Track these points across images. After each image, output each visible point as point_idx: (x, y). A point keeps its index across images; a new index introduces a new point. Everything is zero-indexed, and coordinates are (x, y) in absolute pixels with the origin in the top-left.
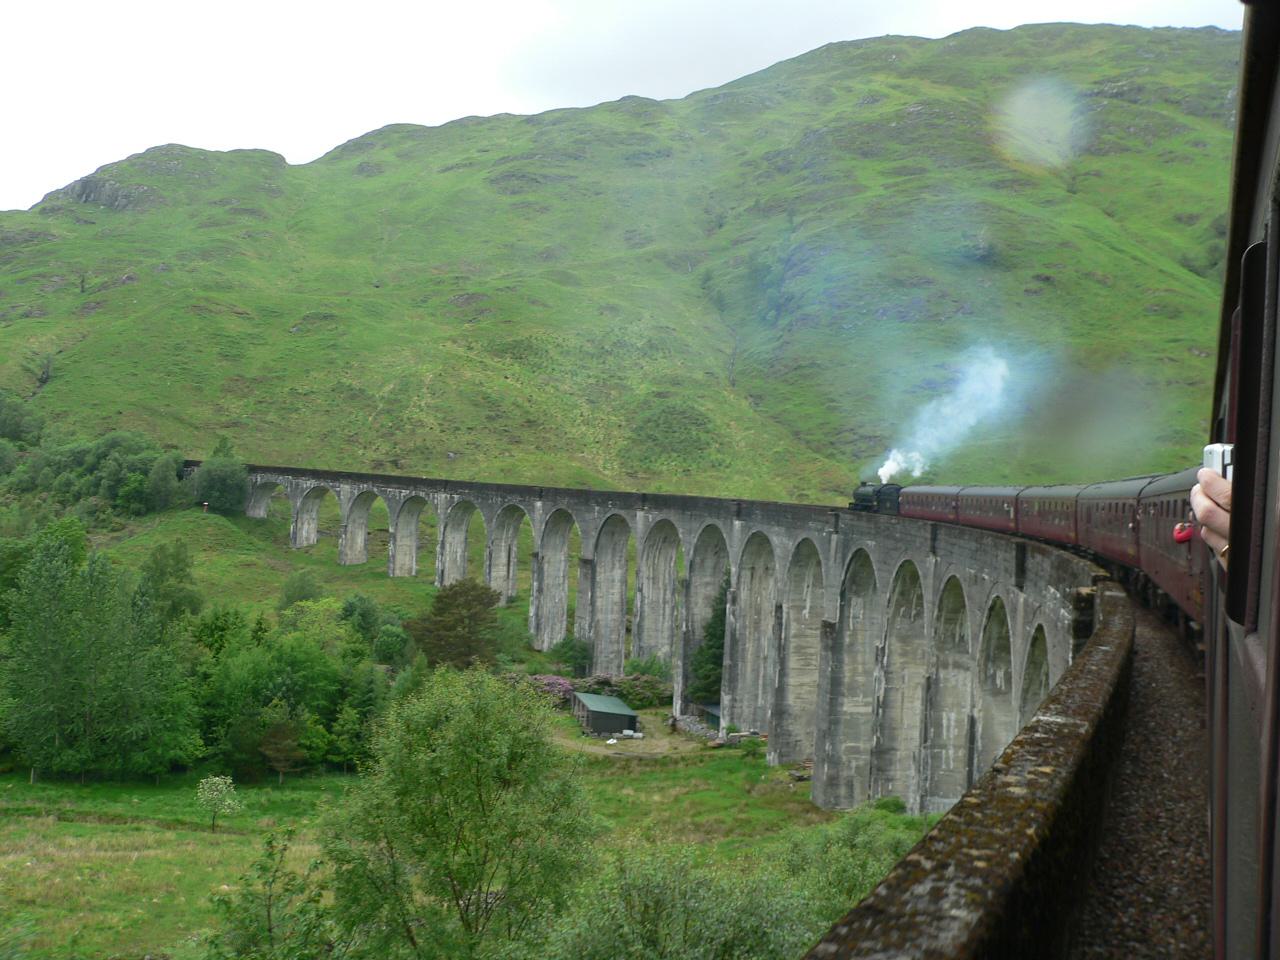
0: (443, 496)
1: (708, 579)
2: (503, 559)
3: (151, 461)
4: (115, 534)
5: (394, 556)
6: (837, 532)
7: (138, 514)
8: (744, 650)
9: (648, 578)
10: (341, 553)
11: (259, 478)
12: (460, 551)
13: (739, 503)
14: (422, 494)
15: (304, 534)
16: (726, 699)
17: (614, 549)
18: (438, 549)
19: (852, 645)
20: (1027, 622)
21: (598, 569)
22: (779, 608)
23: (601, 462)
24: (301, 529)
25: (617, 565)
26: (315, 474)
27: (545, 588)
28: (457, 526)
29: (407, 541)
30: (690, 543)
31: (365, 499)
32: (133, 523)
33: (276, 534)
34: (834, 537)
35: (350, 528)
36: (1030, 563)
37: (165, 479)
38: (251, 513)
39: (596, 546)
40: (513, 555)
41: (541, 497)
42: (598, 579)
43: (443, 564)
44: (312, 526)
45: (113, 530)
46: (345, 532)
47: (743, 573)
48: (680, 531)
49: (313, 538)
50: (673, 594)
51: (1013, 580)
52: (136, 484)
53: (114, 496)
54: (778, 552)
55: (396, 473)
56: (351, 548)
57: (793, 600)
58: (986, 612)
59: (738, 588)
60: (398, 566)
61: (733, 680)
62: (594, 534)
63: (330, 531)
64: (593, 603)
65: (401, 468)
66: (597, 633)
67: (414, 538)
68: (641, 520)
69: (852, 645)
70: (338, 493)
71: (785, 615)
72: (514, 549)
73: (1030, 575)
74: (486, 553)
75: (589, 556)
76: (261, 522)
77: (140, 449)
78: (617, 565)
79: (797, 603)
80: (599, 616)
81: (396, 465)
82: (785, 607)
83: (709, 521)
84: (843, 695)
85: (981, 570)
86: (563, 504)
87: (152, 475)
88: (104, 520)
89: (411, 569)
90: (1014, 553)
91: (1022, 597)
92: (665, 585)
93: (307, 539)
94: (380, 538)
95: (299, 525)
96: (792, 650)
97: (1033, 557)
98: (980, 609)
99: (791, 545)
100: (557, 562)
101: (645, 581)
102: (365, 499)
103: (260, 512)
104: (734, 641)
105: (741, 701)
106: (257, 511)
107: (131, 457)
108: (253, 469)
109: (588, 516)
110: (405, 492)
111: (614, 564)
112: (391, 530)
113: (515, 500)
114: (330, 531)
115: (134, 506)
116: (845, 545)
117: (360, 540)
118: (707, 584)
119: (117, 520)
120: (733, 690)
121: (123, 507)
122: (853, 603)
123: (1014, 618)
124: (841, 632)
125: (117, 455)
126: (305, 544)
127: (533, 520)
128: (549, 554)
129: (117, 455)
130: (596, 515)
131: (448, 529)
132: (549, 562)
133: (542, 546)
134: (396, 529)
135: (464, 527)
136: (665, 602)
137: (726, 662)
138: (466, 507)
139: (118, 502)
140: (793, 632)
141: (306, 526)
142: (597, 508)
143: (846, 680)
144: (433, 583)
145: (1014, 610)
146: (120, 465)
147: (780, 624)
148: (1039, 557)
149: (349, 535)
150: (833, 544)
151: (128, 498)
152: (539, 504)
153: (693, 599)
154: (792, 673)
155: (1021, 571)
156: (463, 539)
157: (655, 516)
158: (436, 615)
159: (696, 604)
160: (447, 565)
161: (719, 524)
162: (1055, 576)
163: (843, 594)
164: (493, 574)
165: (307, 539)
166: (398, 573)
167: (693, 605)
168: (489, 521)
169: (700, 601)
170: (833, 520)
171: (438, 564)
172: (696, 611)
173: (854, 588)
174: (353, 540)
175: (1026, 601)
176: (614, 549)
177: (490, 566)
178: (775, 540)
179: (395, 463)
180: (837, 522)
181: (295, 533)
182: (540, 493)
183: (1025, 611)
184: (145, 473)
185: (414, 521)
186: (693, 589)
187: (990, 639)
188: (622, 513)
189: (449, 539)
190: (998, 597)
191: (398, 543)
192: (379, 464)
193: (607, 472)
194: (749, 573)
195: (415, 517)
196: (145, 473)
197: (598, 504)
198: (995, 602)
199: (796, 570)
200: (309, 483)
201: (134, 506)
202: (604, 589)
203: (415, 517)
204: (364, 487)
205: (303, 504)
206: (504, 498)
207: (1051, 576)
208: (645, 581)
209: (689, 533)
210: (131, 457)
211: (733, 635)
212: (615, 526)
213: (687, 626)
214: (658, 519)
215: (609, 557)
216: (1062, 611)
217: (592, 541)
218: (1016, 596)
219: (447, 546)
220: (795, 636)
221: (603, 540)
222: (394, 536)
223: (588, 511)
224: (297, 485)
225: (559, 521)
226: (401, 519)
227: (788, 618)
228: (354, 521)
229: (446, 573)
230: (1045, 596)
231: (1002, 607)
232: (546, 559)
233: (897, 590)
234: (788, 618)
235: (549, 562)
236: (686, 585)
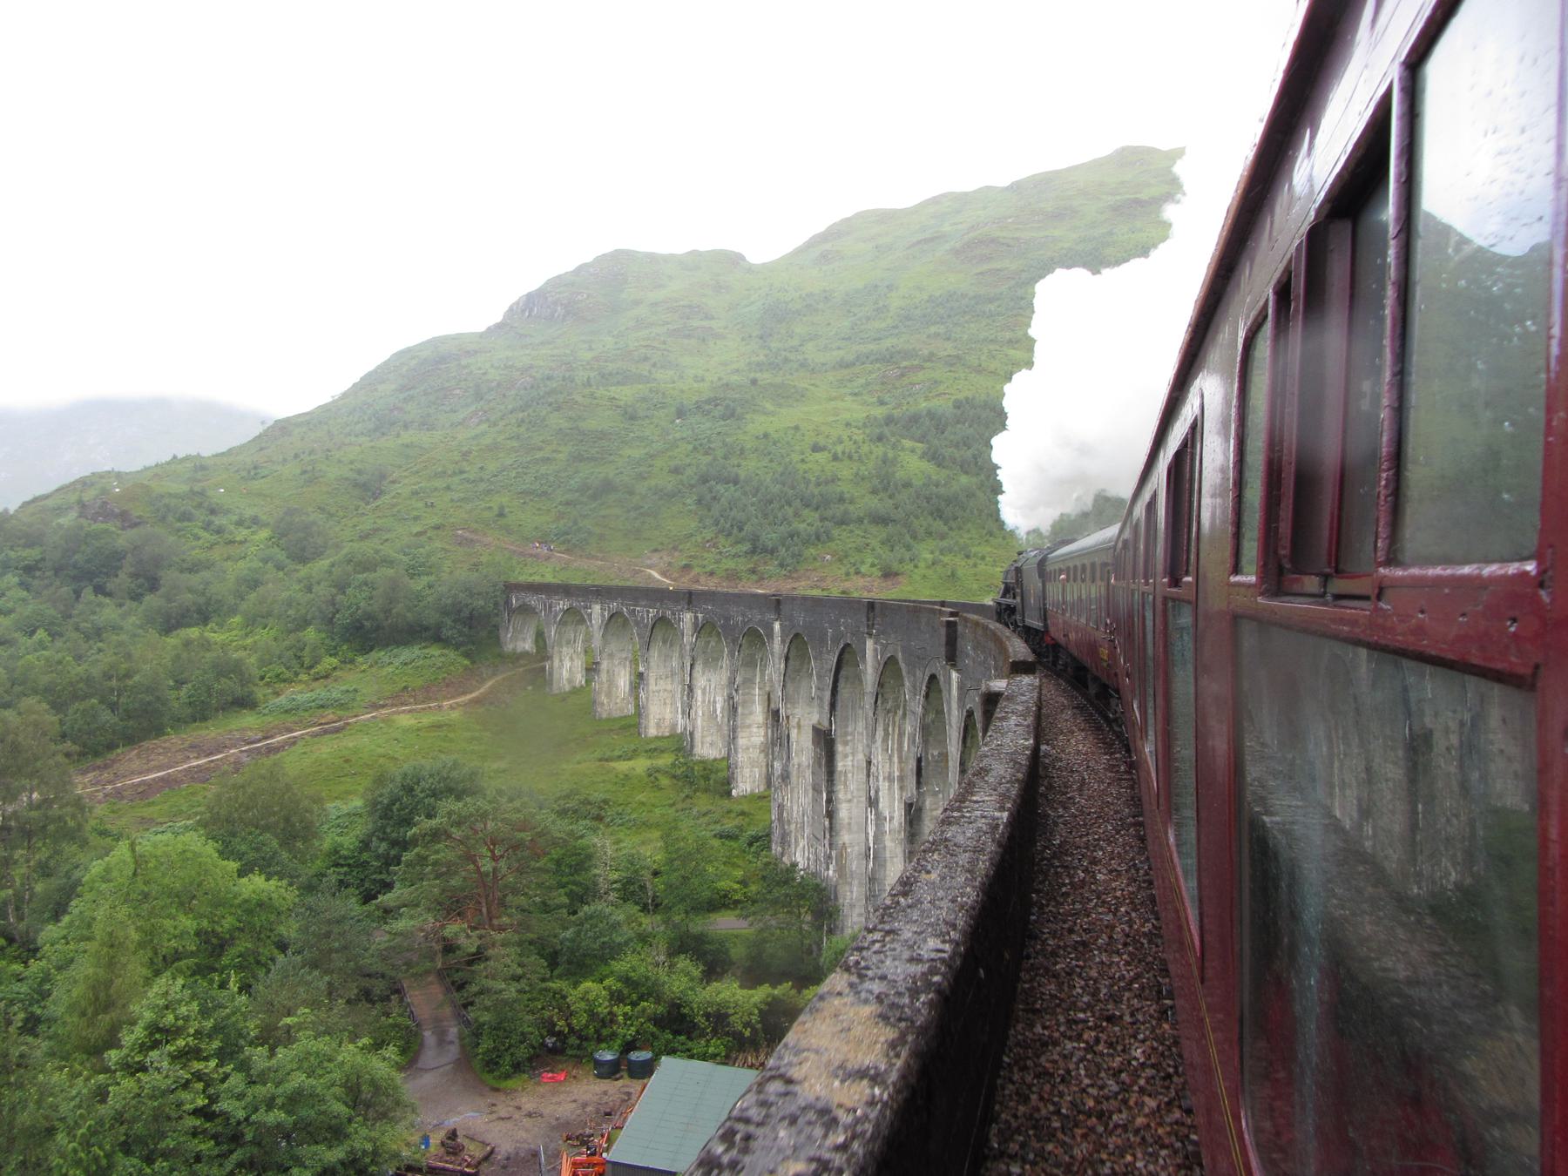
9: (890, 779)
12: (720, 699)
15: (565, 674)
21: (839, 748)
27: (794, 773)
35: (604, 665)
38: (509, 647)
39: (833, 706)
42: (840, 765)
56: (609, 694)
60: (652, 723)
64: (830, 814)
66: (841, 869)
80: (845, 837)
95: (556, 663)
101: (884, 786)
126: (567, 688)
131: (698, 668)
132: (799, 726)
141: (567, 664)
156: (724, 681)
160: (699, 721)
164: (741, 742)
165: (570, 681)
174: (612, 682)
182: (777, 604)
191: (652, 687)
192: (732, 576)
200: (562, 604)
202: (852, 787)
208: (884, 786)
215: (861, 725)
219: (698, 693)
226: (654, 654)
232: (794, 722)
235: (799, 726)
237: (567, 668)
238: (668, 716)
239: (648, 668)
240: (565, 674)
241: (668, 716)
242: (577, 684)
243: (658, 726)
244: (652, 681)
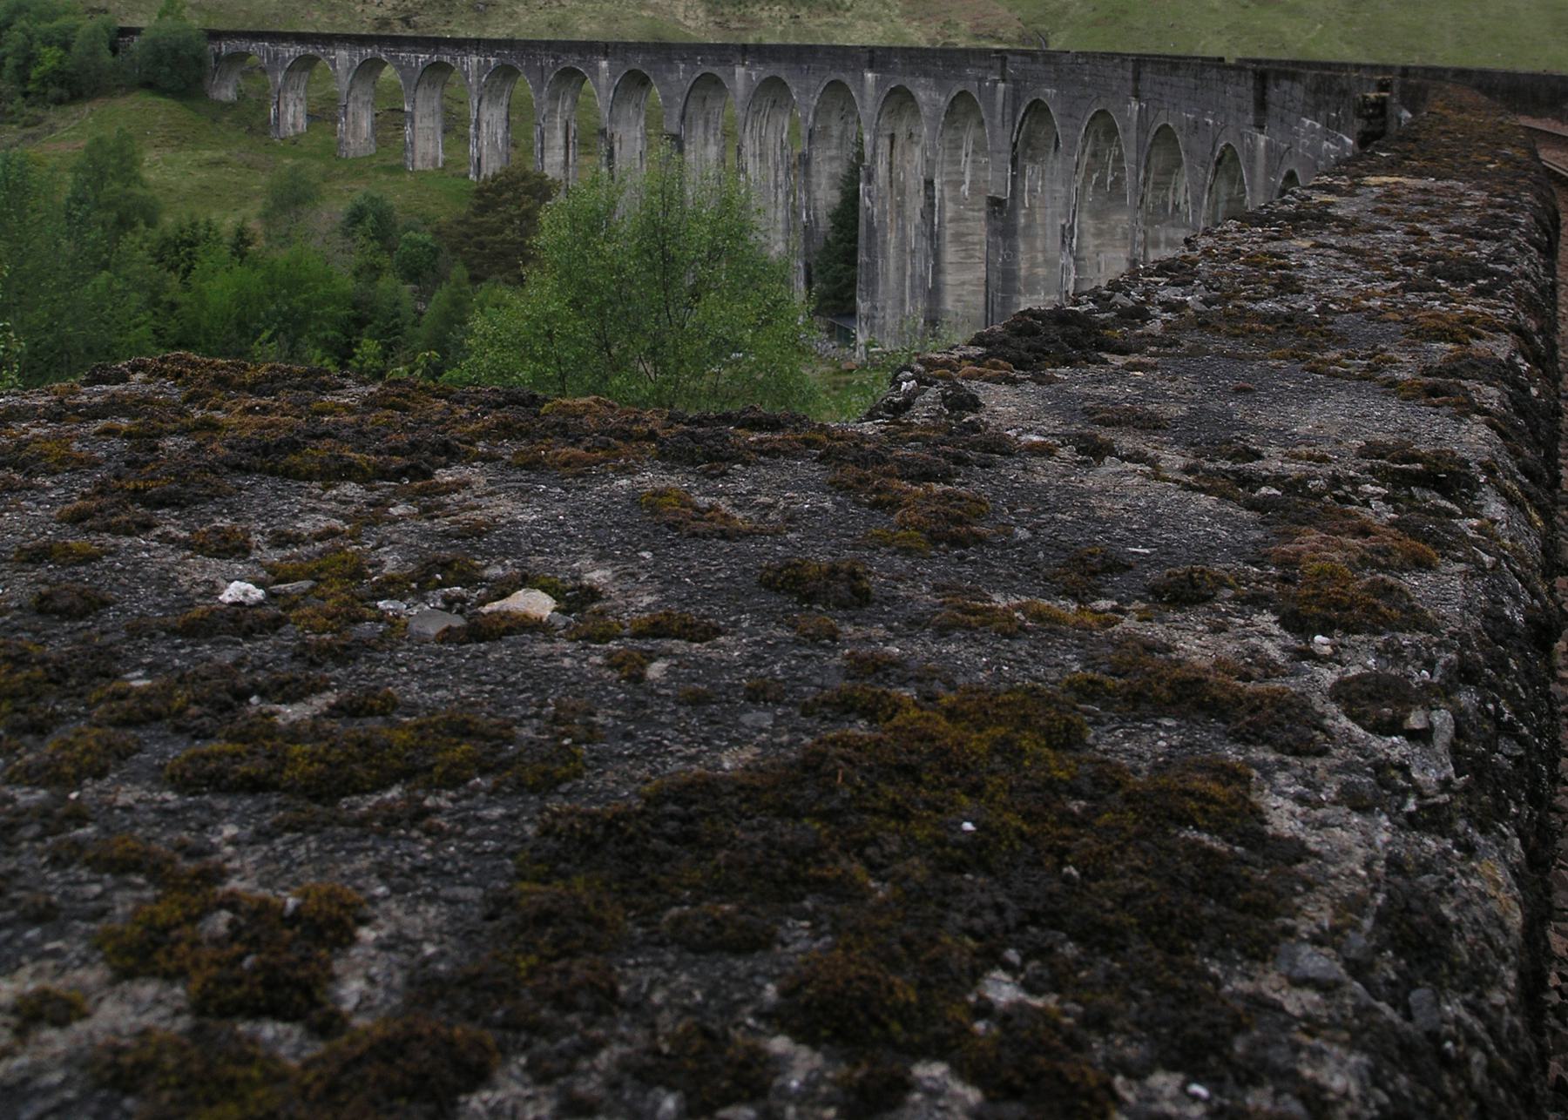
0: (475, 59)
1: (833, 152)
2: (560, 141)
3: (73, 30)
4: (30, 131)
5: (412, 143)
6: (1004, 80)
7: (59, 101)
8: (884, 242)
9: (754, 156)
10: (341, 142)
11: (225, 47)
13: (872, 50)
14: (446, 59)
15: (290, 119)
16: (863, 306)
17: (707, 122)
18: (472, 130)
19: (1028, 226)
20: (1271, 170)
22: (929, 184)
23: (681, 9)
24: (285, 112)
25: (712, 140)
26: (300, 38)
28: (495, 98)
29: (428, 123)
30: (807, 106)
31: (370, 68)
32: (53, 115)
33: (253, 119)
34: (1001, 86)
35: (350, 109)
36: (1273, 94)
37: (93, 53)
39: (683, 118)
40: (572, 134)
41: (606, 55)
43: (479, 150)
44: (300, 108)
45: (26, 125)
46: (346, 115)
47: (880, 141)
48: (794, 90)
49: (302, 122)
50: (787, 175)
51: (1250, 118)
52: (54, 62)
53: (25, 80)
54: (925, 111)
55: (410, 33)
56: (354, 135)
57: (948, 174)
58: (1212, 168)
59: (874, 162)
60: (418, 157)
61: (872, 282)
62: (680, 100)
63: (324, 114)
65: (415, 27)
67: (438, 117)
68: (742, 77)
69: (1028, 226)
70: (333, 63)
71: (937, 194)
72: (573, 125)
73: (1274, 110)
74: (535, 134)
75: (675, 131)
76: (226, 107)
77: (55, 15)
78: (712, 140)
79: (955, 177)
81: (408, 23)
82: (937, 182)
83: (834, 76)
84: (1019, 292)
85: (1204, 112)
86: (637, 62)
87: (75, 49)
88: (12, 113)
89: (435, 159)
90: (1251, 83)
91: (1262, 140)
92: (776, 164)
93: (294, 126)
94: (392, 120)
95: (282, 108)
96: (948, 238)
97: (1277, 86)
98: (1203, 164)
99: (943, 101)
100: (631, 139)
101: (750, 160)
102: (370, 68)
103: (227, 93)
104: (871, 231)
105: (883, 308)
106: (223, 91)
107: (44, 26)
108: (215, 35)
109: (671, 78)
110: (423, 57)
111: (706, 140)
112: (407, 108)
113: (572, 61)
114: (324, 114)
115: (54, 91)
116: (1015, 97)
117: (366, 124)
118: (832, 159)
119: (31, 111)
120: (872, 294)
121: (38, 94)
122: (1028, 172)
123: (1251, 170)
124: (1013, 209)
125: (24, 23)
126: (291, 132)
127: (597, 85)
128: (620, 131)
129: (24, 23)
130: (683, 74)
131: (484, 104)
133: (611, 120)
134: (414, 108)
135: (505, 101)
136: (776, 187)
137: (862, 258)
138: (506, 73)
139: (31, 87)
140: (948, 215)
141: (291, 109)
142: (682, 66)
143: (1023, 273)
144: (466, 176)
145: (1252, 159)
146: (29, 37)
147: (932, 205)
148: (1286, 85)
149: (350, 117)
150: (1000, 96)
151: (44, 81)
152: (604, 64)
153: (814, 180)
154: (949, 269)
155: (1261, 105)
157: (759, 73)
158: (476, 215)
159: (819, 185)
161: (846, 78)
162: (1312, 102)
163: (1014, 162)
164: (547, 160)
165: (294, 126)
166: (419, 165)
167: (814, 187)
168: (539, 90)
169: (824, 181)
170: (998, 64)
171: (472, 150)
172: (819, 194)
173: (1029, 152)
175: (1268, 144)
176: (707, 122)
177: (542, 149)
178: (922, 96)
179: (406, 21)
180: (1004, 66)
181: (277, 118)
183: (1268, 158)
184: (66, 46)
185: (437, 95)
186: (814, 167)
187: (1217, 203)
188: (716, 71)
189: (485, 116)
190: (1228, 146)
191: (418, 124)
192: (384, 22)
193: (689, 23)
194: (887, 142)
195: (439, 89)
196: (66, 46)
197: (683, 60)
198: (1223, 153)
199: (950, 134)
200: (291, 51)
201: (54, 91)
203: (439, 89)
204: (368, 52)
205: (286, 78)
206: (557, 58)
207: (1305, 104)
208: (750, 160)
209: (806, 93)
210: (44, 26)
211: (870, 224)
212: (709, 85)
213: (808, 216)
214: (764, 76)
215: (701, 130)
216: (1325, 144)
217: (677, 112)
218: (1254, 140)
219: (484, 125)
220: (951, 221)
221: (691, 108)
222: (412, 117)
223: (670, 71)
224: (276, 54)
225: (635, 82)
226: (420, 93)
227: (942, 199)
228: (356, 99)
229: (483, 161)
230: (1297, 133)
231: (1235, 158)
232: (617, 137)
233: (1088, 150)
234: (942, 199)
236: (805, 161)
237: (293, 115)
238: (431, 151)
239: (414, 108)
240: (290, 119)
241: (431, 151)
242: (299, 130)
243: (423, 159)
244: (417, 120)
